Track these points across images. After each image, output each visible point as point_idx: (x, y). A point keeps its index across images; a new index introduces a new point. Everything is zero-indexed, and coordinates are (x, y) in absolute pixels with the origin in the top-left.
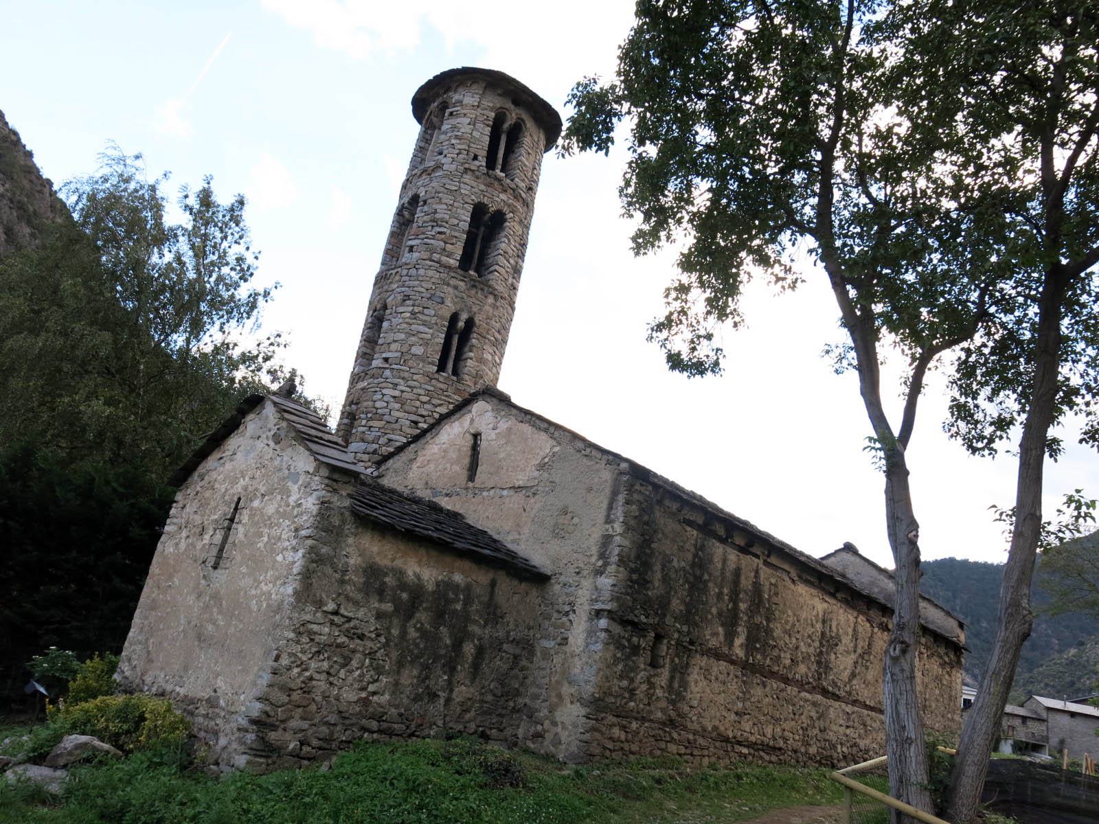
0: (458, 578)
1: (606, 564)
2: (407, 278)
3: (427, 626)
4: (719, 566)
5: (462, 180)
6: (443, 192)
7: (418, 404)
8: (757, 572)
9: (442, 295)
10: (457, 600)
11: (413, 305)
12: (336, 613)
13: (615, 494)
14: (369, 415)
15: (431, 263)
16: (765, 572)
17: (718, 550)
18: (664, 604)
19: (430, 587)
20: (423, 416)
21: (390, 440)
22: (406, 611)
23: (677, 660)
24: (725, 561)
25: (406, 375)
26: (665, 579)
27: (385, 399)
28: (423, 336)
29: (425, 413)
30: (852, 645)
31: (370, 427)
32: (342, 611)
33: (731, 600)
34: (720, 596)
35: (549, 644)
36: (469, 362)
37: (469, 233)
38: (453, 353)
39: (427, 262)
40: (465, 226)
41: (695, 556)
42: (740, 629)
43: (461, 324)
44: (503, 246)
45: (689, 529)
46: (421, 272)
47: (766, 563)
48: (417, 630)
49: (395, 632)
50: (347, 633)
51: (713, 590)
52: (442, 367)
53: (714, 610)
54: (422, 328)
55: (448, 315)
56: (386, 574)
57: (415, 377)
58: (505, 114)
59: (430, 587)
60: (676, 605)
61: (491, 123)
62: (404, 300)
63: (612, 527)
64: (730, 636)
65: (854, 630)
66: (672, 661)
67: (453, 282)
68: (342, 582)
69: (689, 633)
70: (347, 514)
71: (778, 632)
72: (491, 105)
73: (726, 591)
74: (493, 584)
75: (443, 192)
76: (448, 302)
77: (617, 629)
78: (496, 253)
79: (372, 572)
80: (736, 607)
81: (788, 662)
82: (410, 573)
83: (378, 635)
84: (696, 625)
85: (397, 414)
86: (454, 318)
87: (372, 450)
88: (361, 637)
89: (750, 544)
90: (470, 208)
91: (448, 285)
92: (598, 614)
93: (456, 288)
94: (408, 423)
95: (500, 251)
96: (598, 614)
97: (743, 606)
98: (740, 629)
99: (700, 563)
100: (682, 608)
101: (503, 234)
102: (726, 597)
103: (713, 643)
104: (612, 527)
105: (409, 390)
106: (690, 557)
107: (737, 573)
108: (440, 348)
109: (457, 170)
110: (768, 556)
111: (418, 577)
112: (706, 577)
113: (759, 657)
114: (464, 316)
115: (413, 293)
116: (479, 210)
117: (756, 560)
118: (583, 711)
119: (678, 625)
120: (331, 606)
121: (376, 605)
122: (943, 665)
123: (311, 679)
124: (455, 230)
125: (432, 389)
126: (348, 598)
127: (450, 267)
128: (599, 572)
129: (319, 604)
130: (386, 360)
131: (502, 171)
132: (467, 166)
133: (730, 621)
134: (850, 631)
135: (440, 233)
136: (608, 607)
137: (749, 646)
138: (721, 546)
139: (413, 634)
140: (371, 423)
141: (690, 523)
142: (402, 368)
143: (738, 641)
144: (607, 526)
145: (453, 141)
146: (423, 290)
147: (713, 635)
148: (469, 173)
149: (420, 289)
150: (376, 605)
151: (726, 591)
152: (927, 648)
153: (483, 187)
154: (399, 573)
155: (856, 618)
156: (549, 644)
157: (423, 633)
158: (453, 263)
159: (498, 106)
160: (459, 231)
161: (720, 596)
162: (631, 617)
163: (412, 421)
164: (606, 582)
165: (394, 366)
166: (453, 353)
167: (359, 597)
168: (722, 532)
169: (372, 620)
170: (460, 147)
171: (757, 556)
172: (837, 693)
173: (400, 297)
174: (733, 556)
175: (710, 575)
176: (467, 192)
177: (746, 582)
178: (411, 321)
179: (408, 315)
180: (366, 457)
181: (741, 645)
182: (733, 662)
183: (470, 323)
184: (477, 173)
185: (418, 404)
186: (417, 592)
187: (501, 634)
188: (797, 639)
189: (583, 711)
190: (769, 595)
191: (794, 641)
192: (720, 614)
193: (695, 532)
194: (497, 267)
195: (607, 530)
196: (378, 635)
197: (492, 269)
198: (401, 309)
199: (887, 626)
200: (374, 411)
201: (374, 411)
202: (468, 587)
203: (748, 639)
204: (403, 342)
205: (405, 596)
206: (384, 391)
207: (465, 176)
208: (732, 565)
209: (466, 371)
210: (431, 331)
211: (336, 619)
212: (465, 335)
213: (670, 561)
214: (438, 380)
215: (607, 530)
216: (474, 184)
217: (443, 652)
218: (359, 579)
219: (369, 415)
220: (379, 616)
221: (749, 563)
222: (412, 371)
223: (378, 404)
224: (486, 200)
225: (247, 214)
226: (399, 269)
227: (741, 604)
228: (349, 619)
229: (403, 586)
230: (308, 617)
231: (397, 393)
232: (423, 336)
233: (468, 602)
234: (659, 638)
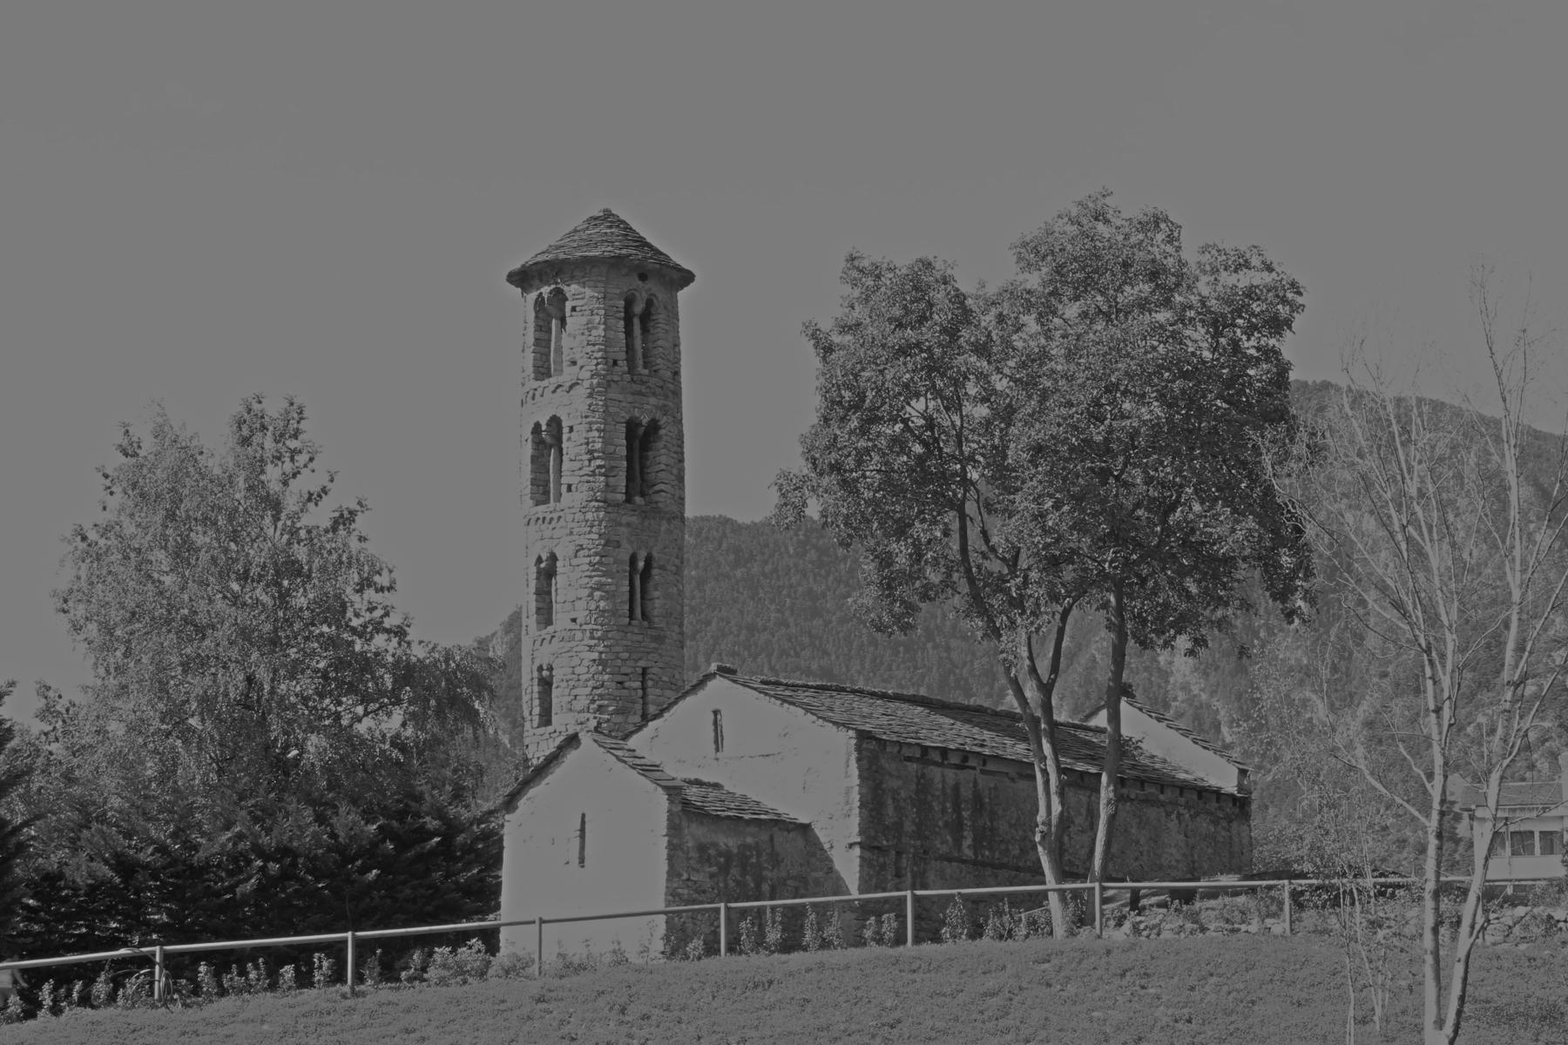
0: (749, 840)
1: (851, 810)
2: (574, 525)
3: (739, 878)
4: (940, 786)
5: (611, 395)
8: (975, 782)
9: (617, 538)
10: (751, 856)
11: (589, 556)
12: (688, 880)
13: (849, 755)
14: (571, 683)
15: (596, 504)
16: (983, 781)
17: (935, 773)
18: (899, 825)
19: (735, 851)
20: (626, 674)
22: (724, 869)
23: (915, 869)
24: (944, 781)
26: (898, 808)
29: (629, 671)
30: (1087, 823)
31: (576, 696)
32: (692, 878)
33: (954, 811)
34: (944, 811)
35: (819, 874)
36: (657, 603)
37: (629, 458)
38: (638, 596)
41: (918, 784)
42: (965, 833)
43: (641, 564)
44: (663, 459)
45: (909, 764)
47: (983, 772)
48: (734, 881)
49: (721, 885)
50: (696, 891)
51: (936, 806)
52: (631, 617)
53: (940, 823)
55: (627, 558)
56: (709, 848)
58: (633, 294)
59: (735, 851)
60: (909, 827)
61: (622, 315)
62: (577, 551)
64: (958, 842)
65: (1088, 810)
66: (912, 871)
67: (625, 520)
68: (689, 859)
69: (922, 846)
70: (680, 814)
71: (1003, 826)
72: (618, 291)
73: (948, 805)
74: (772, 838)
76: (625, 544)
77: (868, 855)
78: (657, 468)
79: (702, 848)
80: (959, 816)
81: (1017, 852)
82: (722, 844)
83: (713, 889)
84: (927, 838)
86: (633, 560)
88: (704, 892)
89: (965, 759)
90: (622, 428)
91: (620, 525)
92: (851, 845)
94: (614, 684)
95: (663, 467)
96: (851, 845)
97: (965, 814)
98: (965, 833)
99: (923, 786)
100: (914, 828)
101: (660, 444)
102: (950, 810)
103: (944, 849)
105: (608, 650)
106: (913, 787)
107: (956, 788)
108: (626, 597)
110: (984, 764)
111: (726, 845)
112: (929, 798)
113: (987, 853)
114: (642, 554)
116: (632, 426)
117: (972, 772)
118: (854, 916)
119: (912, 842)
120: (685, 876)
121: (708, 870)
122: (1215, 822)
123: (684, 923)
124: (615, 459)
125: (629, 643)
126: (693, 869)
129: (680, 875)
130: (574, 620)
131: (645, 367)
132: (609, 378)
133: (957, 828)
134: (1084, 811)
136: (859, 840)
137: (976, 846)
138: (940, 769)
139: (732, 884)
141: (909, 759)
143: (968, 842)
147: (944, 843)
148: (613, 385)
150: (708, 870)
151: (948, 805)
152: (1188, 807)
153: (630, 398)
154: (715, 845)
155: (1089, 797)
156: (819, 874)
157: (738, 883)
158: (621, 497)
159: (626, 290)
161: (944, 811)
162: (876, 844)
163: (618, 683)
164: (854, 823)
166: (638, 596)
167: (699, 866)
168: (938, 759)
169: (708, 880)
171: (974, 768)
172: (1076, 871)
173: (572, 548)
174: (951, 774)
175: (933, 796)
176: (616, 410)
177: (966, 793)
178: (594, 573)
179: (587, 567)
181: (969, 847)
182: (964, 862)
183: (649, 561)
184: (620, 383)
185: (619, 662)
186: (728, 855)
187: (784, 874)
188: (1024, 831)
189: (854, 916)
190: (990, 799)
191: (1021, 833)
192: (946, 824)
193: (915, 766)
194: (662, 487)
196: (713, 889)
198: (575, 562)
199: (1128, 796)
202: (757, 843)
203: (974, 840)
205: (722, 860)
207: (609, 390)
208: (951, 781)
209: (656, 613)
211: (689, 883)
212: (646, 574)
213: (899, 794)
214: (633, 633)
216: (620, 397)
217: (751, 893)
218: (694, 854)
219: (571, 683)
220: (712, 876)
221: (964, 775)
224: (636, 413)
225: (310, 428)
227: (964, 813)
228: (695, 882)
229: (720, 854)
230: (675, 885)
233: (759, 855)
234: (899, 854)
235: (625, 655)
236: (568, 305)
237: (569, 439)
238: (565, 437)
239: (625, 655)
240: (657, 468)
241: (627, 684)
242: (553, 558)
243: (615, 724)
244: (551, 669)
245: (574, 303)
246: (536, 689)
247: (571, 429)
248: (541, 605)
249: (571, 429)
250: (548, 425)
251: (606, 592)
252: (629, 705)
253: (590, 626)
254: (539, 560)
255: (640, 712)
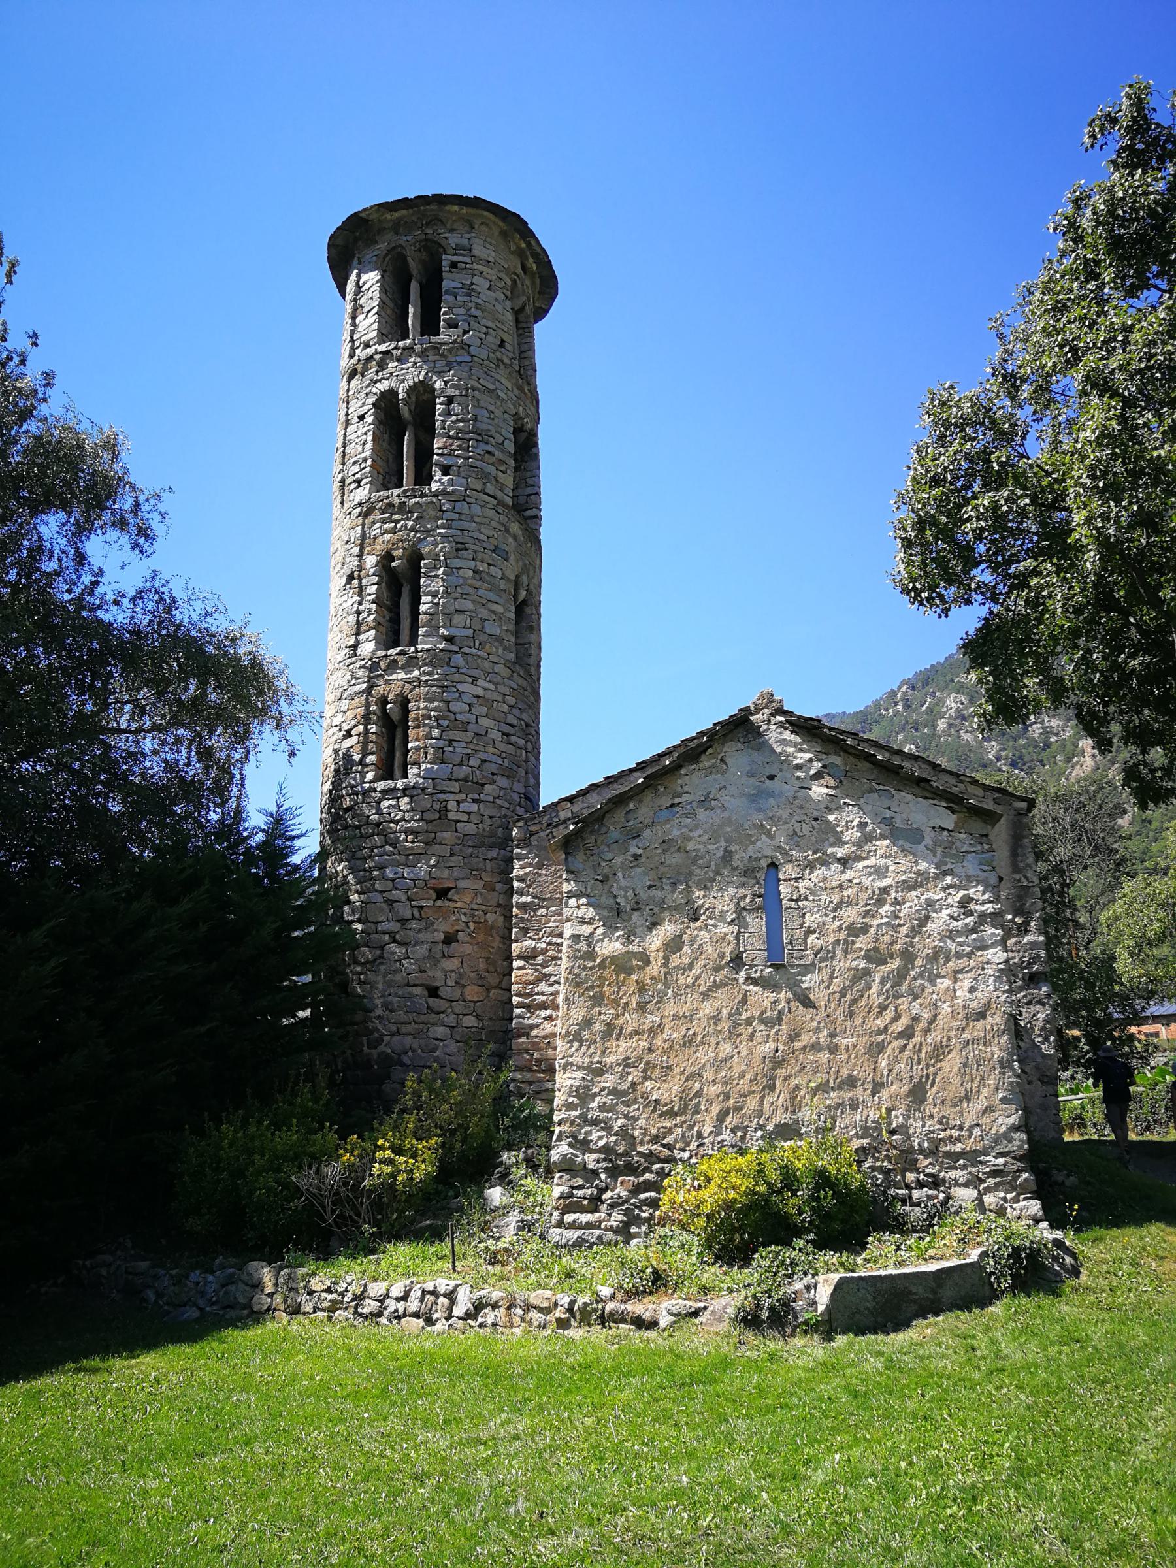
2: (456, 516)
6: (479, 390)
7: (505, 708)
14: (445, 723)
20: (512, 726)
21: (484, 761)
25: (487, 665)
27: (467, 698)
28: (494, 607)
29: (515, 722)
31: (451, 741)
39: (481, 494)
40: (511, 448)
46: (476, 509)
54: (493, 597)
55: (513, 578)
57: (497, 668)
62: (458, 550)
63: (1025, 877)
75: (479, 390)
85: (485, 722)
87: (461, 776)
93: (515, 537)
104: (1025, 877)
109: (488, 359)
115: (472, 541)
125: (516, 687)
127: (500, 503)
128: (1023, 930)
132: (498, 354)
135: (488, 452)
140: (451, 735)
142: (479, 653)
144: (1017, 876)
145: (474, 311)
146: (483, 537)
149: (476, 535)
160: (503, 452)
163: (504, 734)
165: (466, 650)
170: (484, 322)
179: (471, 573)
180: (456, 786)
185: (505, 708)
195: (1019, 881)
197: (528, 513)
200: (452, 717)
201: (452, 717)
204: (472, 616)
206: (461, 687)
210: (501, 601)
215: (1019, 881)
219: (445, 723)
222: (492, 658)
223: (454, 707)
226: (434, 499)
231: (480, 692)
232: (494, 607)
235: (512, 701)
236: (446, 260)
237: (448, 413)
238: (440, 408)
239: (512, 701)
240: (529, 490)
241: (513, 739)
242: (414, 558)
243: (501, 788)
244: (404, 702)
245: (455, 258)
246: (373, 728)
247: (450, 401)
248: (381, 620)
249: (450, 401)
250: (409, 392)
251: (493, 612)
252: (515, 767)
253: (473, 651)
254: (387, 557)
255: (523, 780)
